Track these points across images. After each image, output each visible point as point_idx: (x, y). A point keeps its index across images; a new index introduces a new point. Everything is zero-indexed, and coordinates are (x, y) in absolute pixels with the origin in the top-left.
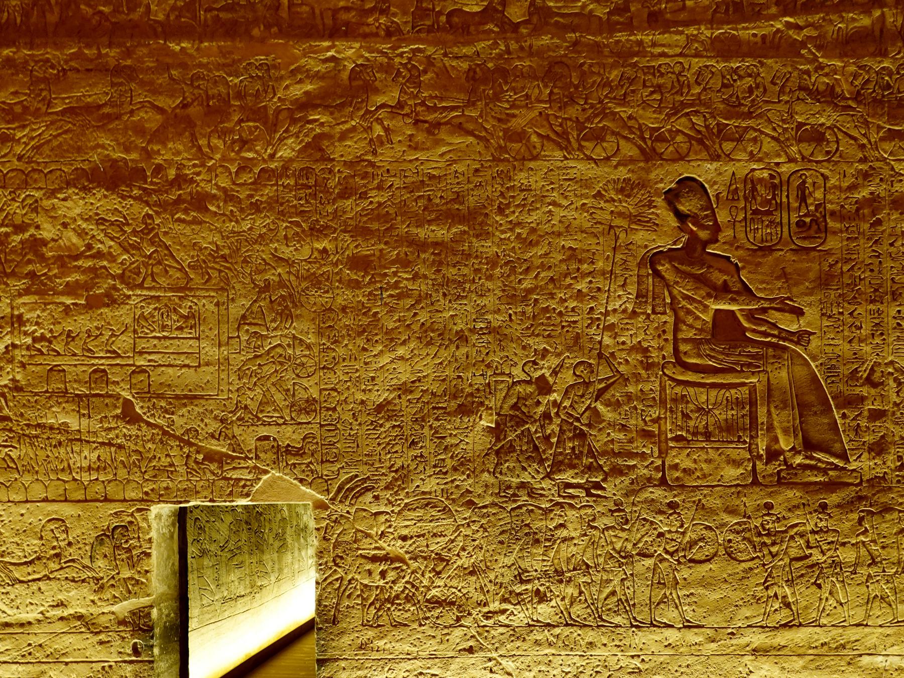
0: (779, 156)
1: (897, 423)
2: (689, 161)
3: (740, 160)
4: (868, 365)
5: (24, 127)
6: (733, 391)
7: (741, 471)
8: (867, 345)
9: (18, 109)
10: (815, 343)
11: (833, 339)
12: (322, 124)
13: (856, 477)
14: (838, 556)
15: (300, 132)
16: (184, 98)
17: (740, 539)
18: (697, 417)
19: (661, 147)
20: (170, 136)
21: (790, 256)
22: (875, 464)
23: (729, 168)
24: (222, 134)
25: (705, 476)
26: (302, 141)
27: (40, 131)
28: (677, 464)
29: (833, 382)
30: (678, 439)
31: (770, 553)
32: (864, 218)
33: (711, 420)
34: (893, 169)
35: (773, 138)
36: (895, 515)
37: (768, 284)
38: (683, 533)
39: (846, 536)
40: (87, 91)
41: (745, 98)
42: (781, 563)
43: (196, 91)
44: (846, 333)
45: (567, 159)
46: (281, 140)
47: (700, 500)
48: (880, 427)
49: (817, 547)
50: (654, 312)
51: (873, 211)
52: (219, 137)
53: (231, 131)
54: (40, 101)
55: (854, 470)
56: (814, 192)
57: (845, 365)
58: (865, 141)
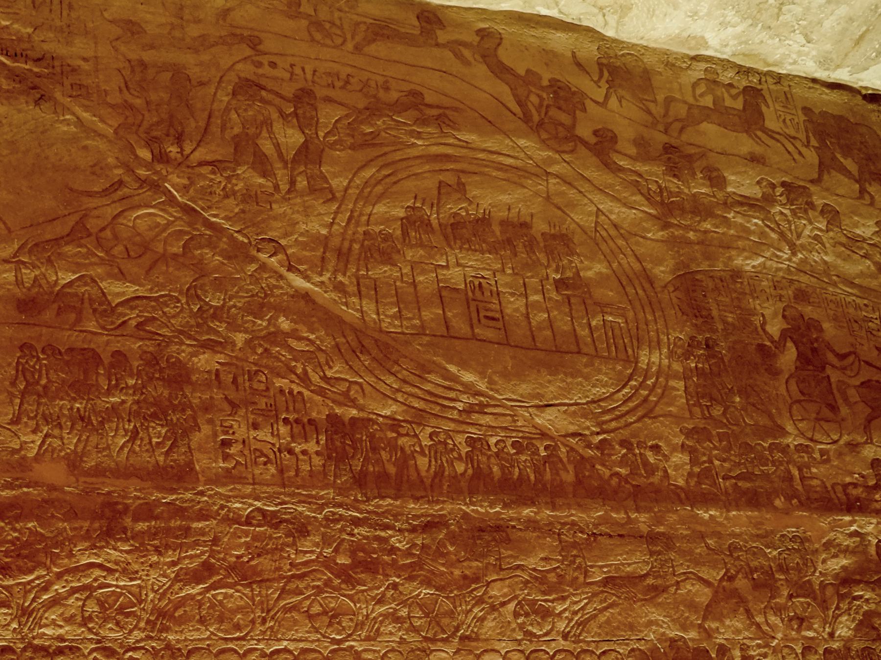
5: (564, 599)
9: (552, 578)
12: (867, 600)
15: (850, 609)
16: (728, 571)
20: (725, 612)
24: (778, 610)
26: (854, 618)
27: (583, 604)
40: (625, 559)
43: (737, 563)
46: (836, 617)
52: (776, 615)
53: (785, 608)
54: (575, 570)
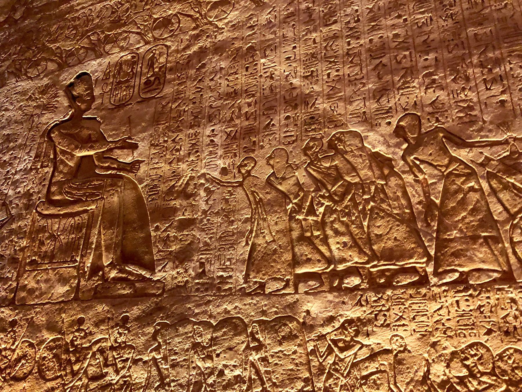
0: (139, 42)
1: (203, 230)
2: (84, 63)
3: (114, 53)
4: (184, 180)
6: (76, 218)
7: (67, 288)
8: (183, 163)
10: (143, 168)
11: (158, 163)
13: (158, 288)
14: (130, 376)
17: (51, 356)
18: (49, 243)
19: (70, 61)
21: (136, 107)
22: (178, 273)
23: (106, 61)
25: (41, 294)
28: (26, 285)
29: (153, 200)
30: (33, 262)
31: (72, 370)
32: (193, 67)
33: (58, 244)
34: (217, 27)
35: (137, 33)
36: (189, 328)
37: (116, 130)
38: (14, 351)
39: (140, 353)
41: (122, 16)
42: (79, 383)
44: (168, 156)
45: (17, 81)
47: (33, 317)
48: (187, 235)
49: (112, 365)
50: (42, 167)
51: (200, 60)
55: (158, 281)
56: (159, 59)
57: (164, 183)
58: (198, 15)
